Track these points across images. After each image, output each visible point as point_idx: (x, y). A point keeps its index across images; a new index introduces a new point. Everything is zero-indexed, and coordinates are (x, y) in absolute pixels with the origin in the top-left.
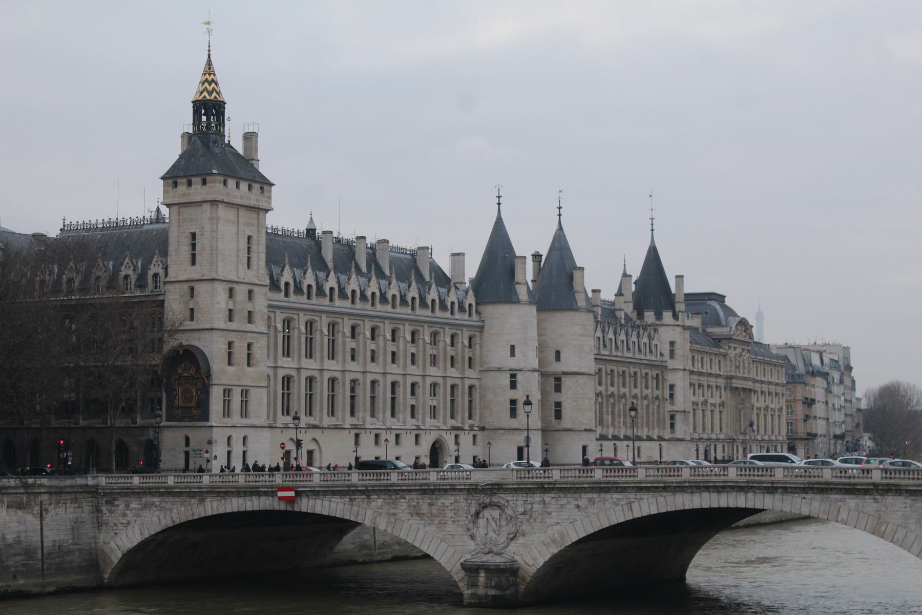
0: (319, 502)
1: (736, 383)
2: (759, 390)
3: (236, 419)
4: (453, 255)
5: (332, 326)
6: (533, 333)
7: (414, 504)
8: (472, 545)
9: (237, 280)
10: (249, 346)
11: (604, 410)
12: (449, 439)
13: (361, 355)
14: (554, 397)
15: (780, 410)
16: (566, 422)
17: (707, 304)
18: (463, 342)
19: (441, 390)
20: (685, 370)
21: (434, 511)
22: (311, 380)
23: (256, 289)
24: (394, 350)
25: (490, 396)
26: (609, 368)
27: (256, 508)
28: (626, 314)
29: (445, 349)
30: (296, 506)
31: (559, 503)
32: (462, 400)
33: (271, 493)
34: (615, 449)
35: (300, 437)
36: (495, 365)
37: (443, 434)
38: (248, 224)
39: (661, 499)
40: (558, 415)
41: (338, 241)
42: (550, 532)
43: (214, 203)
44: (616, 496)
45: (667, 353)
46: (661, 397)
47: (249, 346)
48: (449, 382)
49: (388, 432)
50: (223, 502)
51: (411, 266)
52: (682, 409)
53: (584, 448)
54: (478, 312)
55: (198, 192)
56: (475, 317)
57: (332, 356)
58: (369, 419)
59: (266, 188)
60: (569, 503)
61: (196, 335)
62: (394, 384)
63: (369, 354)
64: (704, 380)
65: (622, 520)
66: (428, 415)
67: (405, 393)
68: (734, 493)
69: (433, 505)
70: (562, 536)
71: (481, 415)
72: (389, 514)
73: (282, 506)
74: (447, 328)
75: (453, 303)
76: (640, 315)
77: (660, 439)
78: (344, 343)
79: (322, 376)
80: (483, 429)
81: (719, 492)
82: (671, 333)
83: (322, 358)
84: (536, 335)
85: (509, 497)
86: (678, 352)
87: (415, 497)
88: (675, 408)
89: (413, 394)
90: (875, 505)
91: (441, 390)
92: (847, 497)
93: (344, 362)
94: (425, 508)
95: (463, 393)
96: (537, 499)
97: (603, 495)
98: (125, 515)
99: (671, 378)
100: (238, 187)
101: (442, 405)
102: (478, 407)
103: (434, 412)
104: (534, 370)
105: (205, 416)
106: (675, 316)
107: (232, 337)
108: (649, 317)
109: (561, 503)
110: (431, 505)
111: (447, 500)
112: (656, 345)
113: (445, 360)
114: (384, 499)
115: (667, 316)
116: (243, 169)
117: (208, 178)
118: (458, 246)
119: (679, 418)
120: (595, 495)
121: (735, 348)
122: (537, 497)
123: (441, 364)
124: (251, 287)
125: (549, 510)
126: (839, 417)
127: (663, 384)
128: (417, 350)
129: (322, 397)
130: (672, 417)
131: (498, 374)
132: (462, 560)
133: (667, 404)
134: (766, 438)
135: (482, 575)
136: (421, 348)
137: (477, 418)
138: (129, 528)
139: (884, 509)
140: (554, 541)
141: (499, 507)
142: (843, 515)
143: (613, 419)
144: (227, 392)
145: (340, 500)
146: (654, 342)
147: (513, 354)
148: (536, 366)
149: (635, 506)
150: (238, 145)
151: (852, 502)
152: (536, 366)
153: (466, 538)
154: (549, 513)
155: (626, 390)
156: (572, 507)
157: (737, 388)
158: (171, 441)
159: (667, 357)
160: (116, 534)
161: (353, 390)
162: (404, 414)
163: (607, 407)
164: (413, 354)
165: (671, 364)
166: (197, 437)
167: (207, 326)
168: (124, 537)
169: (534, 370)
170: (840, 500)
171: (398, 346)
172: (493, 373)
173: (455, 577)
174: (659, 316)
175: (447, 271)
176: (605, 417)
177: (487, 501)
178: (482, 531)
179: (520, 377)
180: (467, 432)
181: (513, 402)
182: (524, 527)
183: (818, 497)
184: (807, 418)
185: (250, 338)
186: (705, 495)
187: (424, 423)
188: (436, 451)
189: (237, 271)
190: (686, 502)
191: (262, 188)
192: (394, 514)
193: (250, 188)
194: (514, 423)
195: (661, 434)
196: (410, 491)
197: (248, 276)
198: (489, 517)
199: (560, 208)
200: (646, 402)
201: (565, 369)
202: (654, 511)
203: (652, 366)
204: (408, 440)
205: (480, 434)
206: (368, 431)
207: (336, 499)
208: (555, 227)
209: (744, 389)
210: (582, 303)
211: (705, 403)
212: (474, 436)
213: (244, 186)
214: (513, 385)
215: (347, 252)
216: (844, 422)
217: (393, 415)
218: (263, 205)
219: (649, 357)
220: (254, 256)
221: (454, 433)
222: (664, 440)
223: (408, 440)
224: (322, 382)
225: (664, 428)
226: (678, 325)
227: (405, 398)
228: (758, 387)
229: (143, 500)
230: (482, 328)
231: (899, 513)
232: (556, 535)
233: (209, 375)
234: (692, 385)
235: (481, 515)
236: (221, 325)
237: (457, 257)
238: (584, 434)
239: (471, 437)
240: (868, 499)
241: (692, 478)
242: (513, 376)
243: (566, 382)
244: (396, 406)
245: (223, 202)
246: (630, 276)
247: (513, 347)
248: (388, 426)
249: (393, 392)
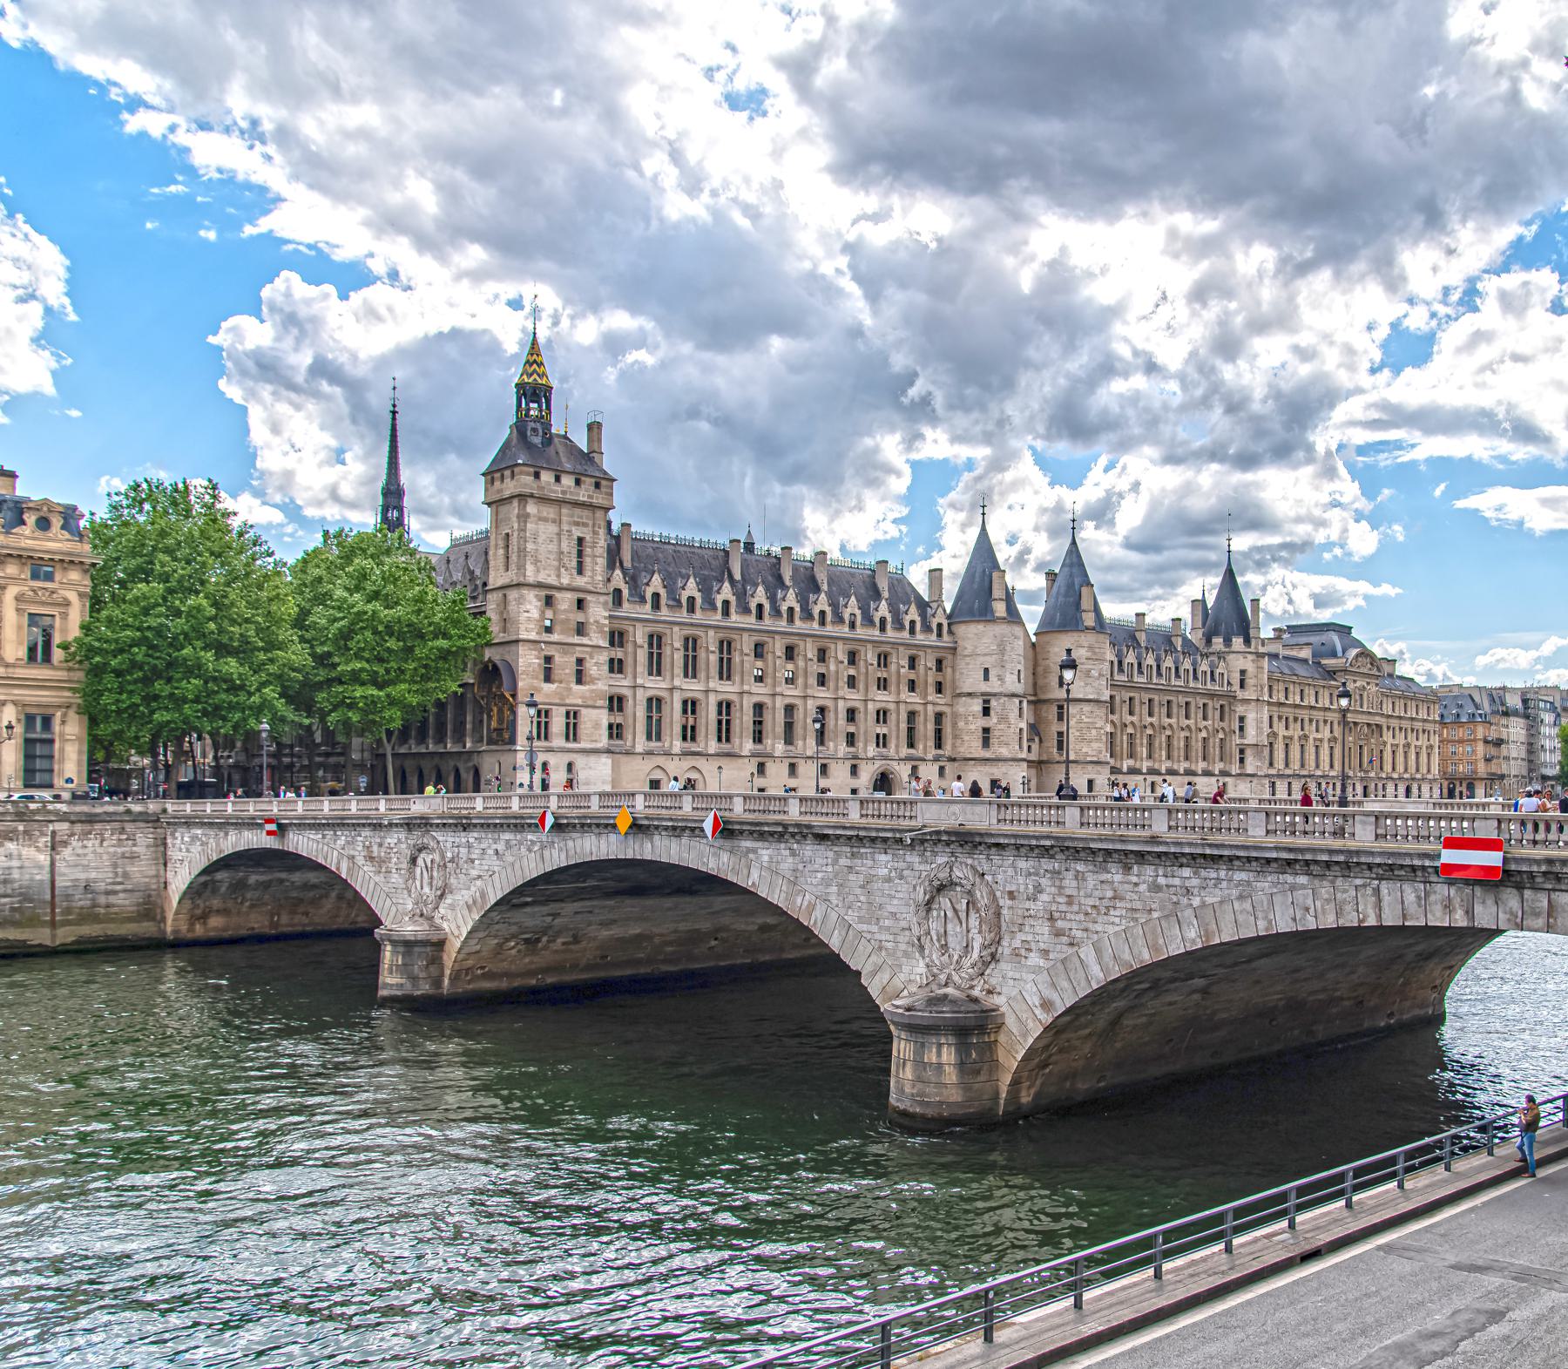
3: (558, 741)
5: (726, 646)
9: (556, 583)
10: (580, 661)
12: (903, 771)
15: (1431, 747)
22: (759, 708)
23: (589, 598)
24: (822, 671)
25: (961, 724)
26: (1146, 697)
32: (926, 728)
36: (966, 690)
38: (577, 524)
43: (522, 498)
47: (580, 661)
54: (950, 632)
55: (509, 487)
59: (604, 483)
61: (507, 648)
62: (822, 710)
64: (1305, 714)
74: (901, 649)
76: (1209, 642)
80: (954, 760)
86: (1250, 682)
93: (742, 683)
99: (1240, 709)
100: (558, 479)
101: (894, 734)
103: (882, 741)
105: (513, 741)
106: (1247, 641)
107: (550, 651)
115: (1238, 642)
116: (586, 465)
117: (516, 470)
119: (1248, 752)
123: (893, 688)
124: (581, 595)
130: (1242, 752)
131: (968, 700)
136: (863, 670)
144: (543, 716)
147: (986, 678)
150: (581, 441)
155: (1173, 721)
157: (1356, 724)
158: (489, 766)
159: (1236, 687)
165: (1240, 694)
166: (506, 759)
167: (514, 638)
174: (1228, 642)
179: (994, 703)
181: (986, 730)
185: (579, 652)
188: (884, 782)
189: (559, 576)
191: (597, 485)
193: (578, 482)
194: (988, 755)
197: (581, 581)
203: (1212, 695)
204: (839, 772)
205: (949, 767)
208: (1069, 540)
210: (1089, 619)
211: (1306, 737)
212: (942, 769)
213: (568, 481)
214: (986, 711)
218: (598, 499)
219: (1209, 686)
220: (588, 560)
222: (1229, 775)
223: (839, 772)
227: (837, 723)
233: (514, 696)
236: (533, 636)
238: (1090, 767)
242: (986, 702)
243: (1073, 709)
245: (532, 496)
247: (986, 670)
248: (809, 753)
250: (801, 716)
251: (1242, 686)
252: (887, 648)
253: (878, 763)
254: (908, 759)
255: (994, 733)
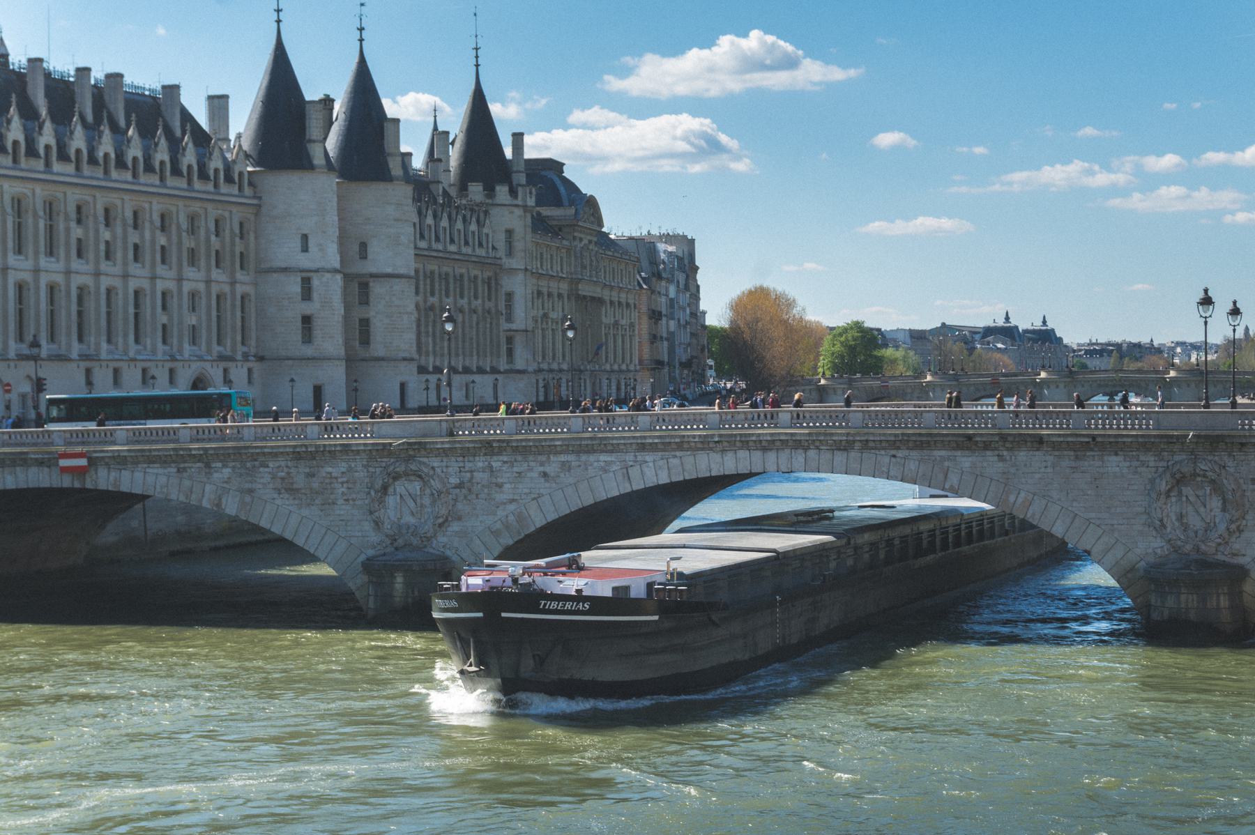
0: (126, 474)
1: (586, 290)
2: (607, 298)
4: (211, 98)
6: (333, 218)
7: (283, 474)
8: (374, 538)
11: (423, 329)
12: (216, 373)
13: (91, 248)
14: (359, 313)
16: (377, 349)
17: (547, 175)
18: (232, 229)
19: (204, 302)
20: (526, 270)
21: (316, 485)
27: (23, 485)
28: (445, 191)
29: (208, 240)
30: (88, 480)
31: (515, 469)
33: (48, 462)
34: (495, 386)
35: (41, 375)
37: (207, 365)
39: (675, 462)
40: (365, 340)
41: (48, 75)
42: (501, 513)
44: (604, 457)
45: (501, 245)
46: (493, 310)
48: (215, 289)
49: (132, 364)
51: (155, 113)
52: (523, 327)
53: (403, 386)
56: (248, 191)
57: (51, 252)
58: (104, 345)
60: (531, 470)
63: (102, 247)
65: (615, 493)
66: (186, 339)
67: (154, 308)
68: (787, 451)
69: (313, 475)
70: (520, 518)
71: (258, 338)
72: (242, 491)
73: (67, 482)
75: (216, 171)
77: (494, 371)
78: (68, 230)
79: (37, 281)
80: (261, 359)
81: (765, 449)
82: (509, 216)
83: (36, 253)
84: (336, 218)
85: (435, 463)
86: (518, 246)
87: (283, 464)
88: (514, 326)
89: (164, 307)
90: (1001, 464)
91: (204, 302)
92: (959, 453)
94: (300, 481)
95: (233, 306)
96: (480, 464)
97: (584, 457)
102: (253, 327)
104: (336, 271)
106: (513, 192)
108: (476, 191)
109: (515, 469)
110: (311, 475)
111: (337, 469)
112: (487, 235)
113: (208, 257)
114: (234, 467)
115: (502, 191)
118: (220, 83)
119: (519, 341)
120: (571, 458)
121: (581, 240)
122: (480, 462)
123: (203, 263)
125: (500, 480)
126: (683, 337)
127: (497, 290)
128: (169, 240)
129: (38, 315)
132: (362, 558)
133: (502, 320)
134: (616, 367)
135: (399, 579)
136: (175, 238)
137: (253, 343)
139: (1013, 470)
140: (507, 527)
141: (420, 477)
142: (954, 479)
143: (435, 344)
145: (161, 471)
146: (485, 230)
147: (305, 249)
148: (337, 265)
149: (635, 472)
151: (966, 461)
152: (337, 265)
153: (368, 526)
154: (500, 486)
156: (535, 475)
157: (585, 297)
159: (501, 253)
161: (20, 299)
162: (152, 339)
163: (427, 326)
164: (163, 248)
165: (509, 263)
169: (336, 271)
170: (949, 459)
171: (142, 237)
172: (275, 275)
173: (350, 584)
174: (490, 191)
175: (202, 119)
176: (423, 340)
177: (401, 468)
178: (391, 513)
179: (316, 282)
180: (239, 364)
181: (307, 320)
182: (460, 506)
183: (915, 454)
184: (654, 338)
186: (743, 454)
187: (180, 351)
190: (713, 466)
192: (251, 491)
194: (309, 351)
195: (494, 364)
196: (275, 455)
198: (404, 492)
199: (361, 29)
200: (475, 317)
201: (373, 270)
202: (664, 479)
203: (481, 263)
205: (256, 366)
206: (104, 364)
207: (155, 469)
208: (356, 59)
209: (593, 298)
210: (396, 170)
211: (545, 316)
214: (307, 294)
215: (63, 92)
216: (689, 344)
217: (137, 341)
221: (223, 365)
222: (499, 372)
224: (37, 288)
225: (499, 356)
226: (516, 206)
228: (606, 295)
230: (260, 206)
231: (1037, 476)
232: (511, 518)
234: (539, 293)
235: (391, 490)
237: (219, 104)
238: (402, 365)
239: (245, 370)
240: (990, 456)
243: (377, 289)
244: (141, 325)
246: (447, 133)
247: (305, 238)
248: (131, 354)
249: (137, 306)
250: (120, 303)
251: (510, 252)
252: (196, 207)
253: (195, 366)
254: (222, 358)
255: (317, 324)
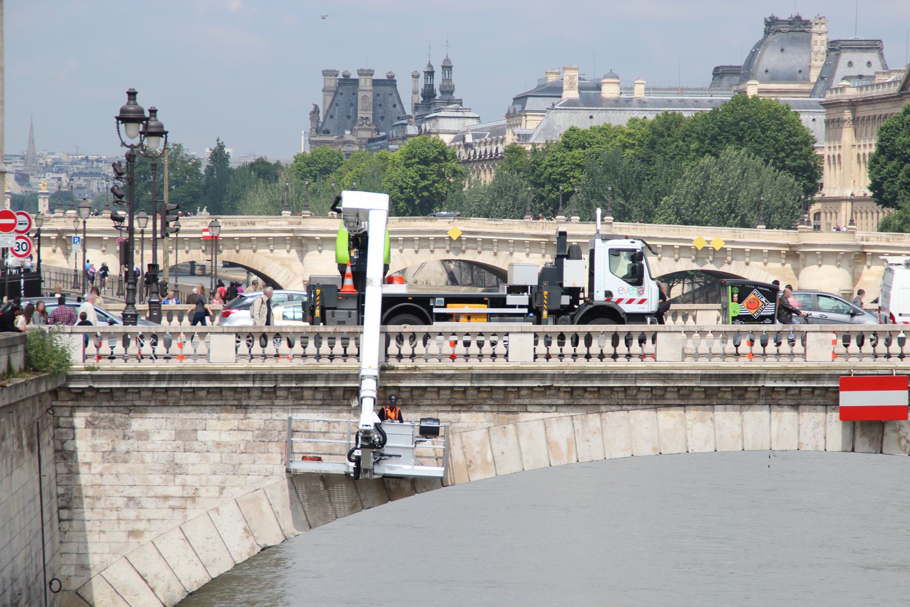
50: (594, 420)
98: (173, 469)
138: (192, 513)
160: (133, 533)
168: (172, 546)
229: (257, 418)
241: (243, 365)
